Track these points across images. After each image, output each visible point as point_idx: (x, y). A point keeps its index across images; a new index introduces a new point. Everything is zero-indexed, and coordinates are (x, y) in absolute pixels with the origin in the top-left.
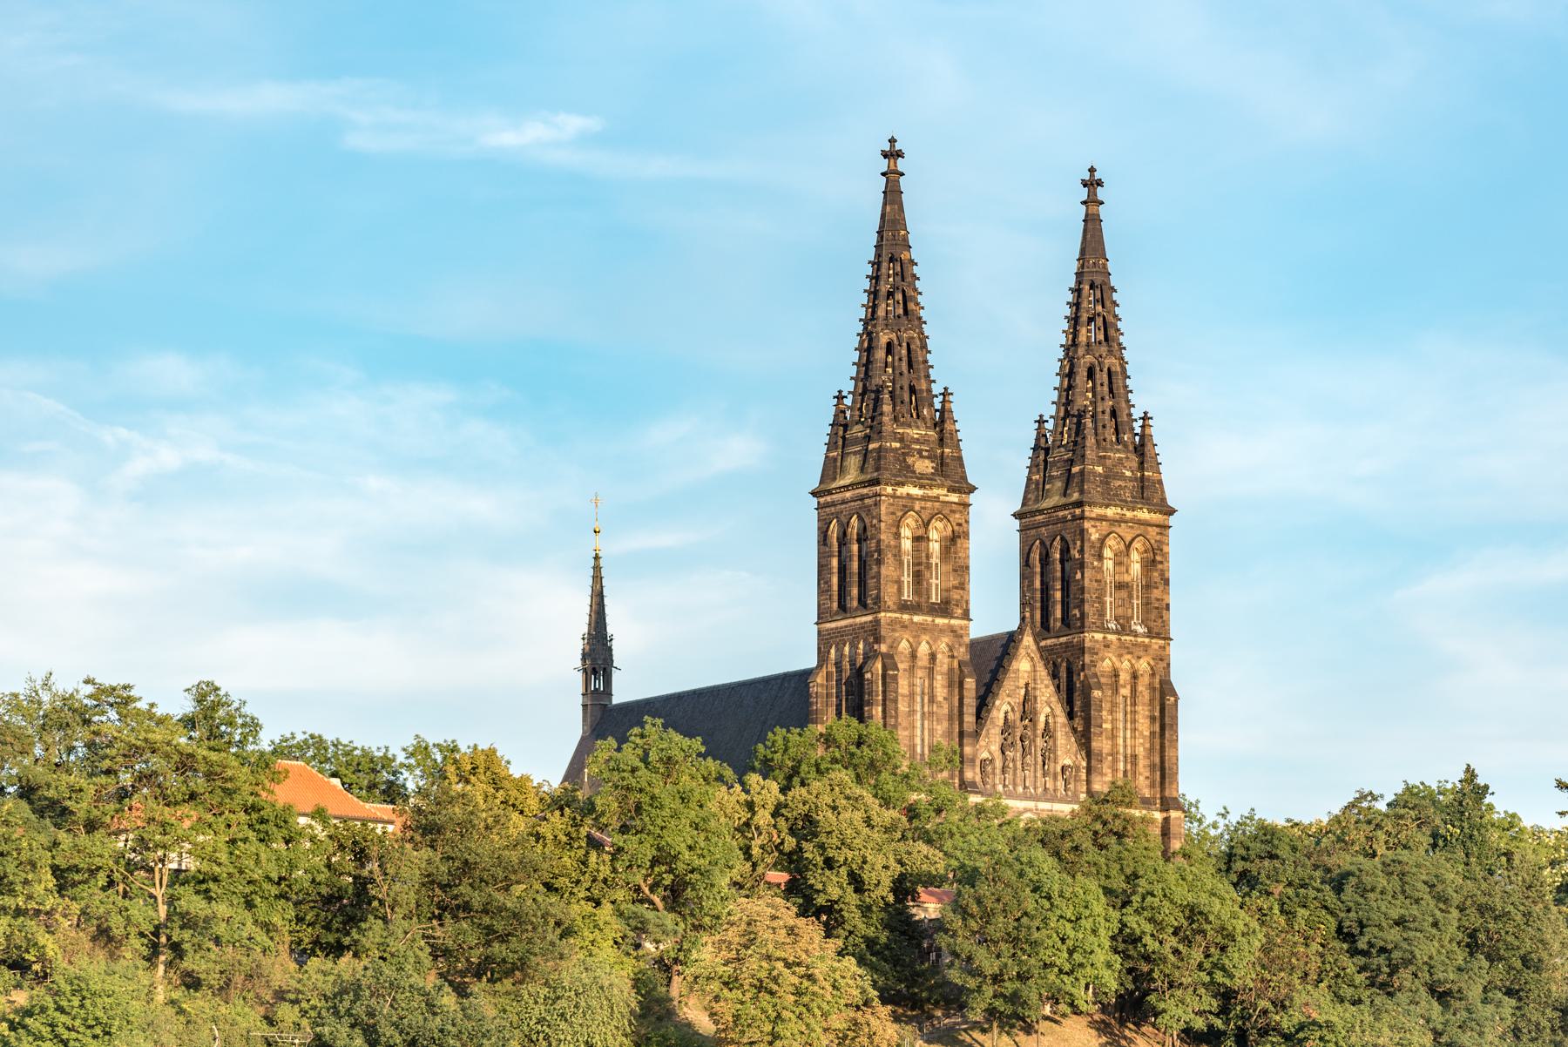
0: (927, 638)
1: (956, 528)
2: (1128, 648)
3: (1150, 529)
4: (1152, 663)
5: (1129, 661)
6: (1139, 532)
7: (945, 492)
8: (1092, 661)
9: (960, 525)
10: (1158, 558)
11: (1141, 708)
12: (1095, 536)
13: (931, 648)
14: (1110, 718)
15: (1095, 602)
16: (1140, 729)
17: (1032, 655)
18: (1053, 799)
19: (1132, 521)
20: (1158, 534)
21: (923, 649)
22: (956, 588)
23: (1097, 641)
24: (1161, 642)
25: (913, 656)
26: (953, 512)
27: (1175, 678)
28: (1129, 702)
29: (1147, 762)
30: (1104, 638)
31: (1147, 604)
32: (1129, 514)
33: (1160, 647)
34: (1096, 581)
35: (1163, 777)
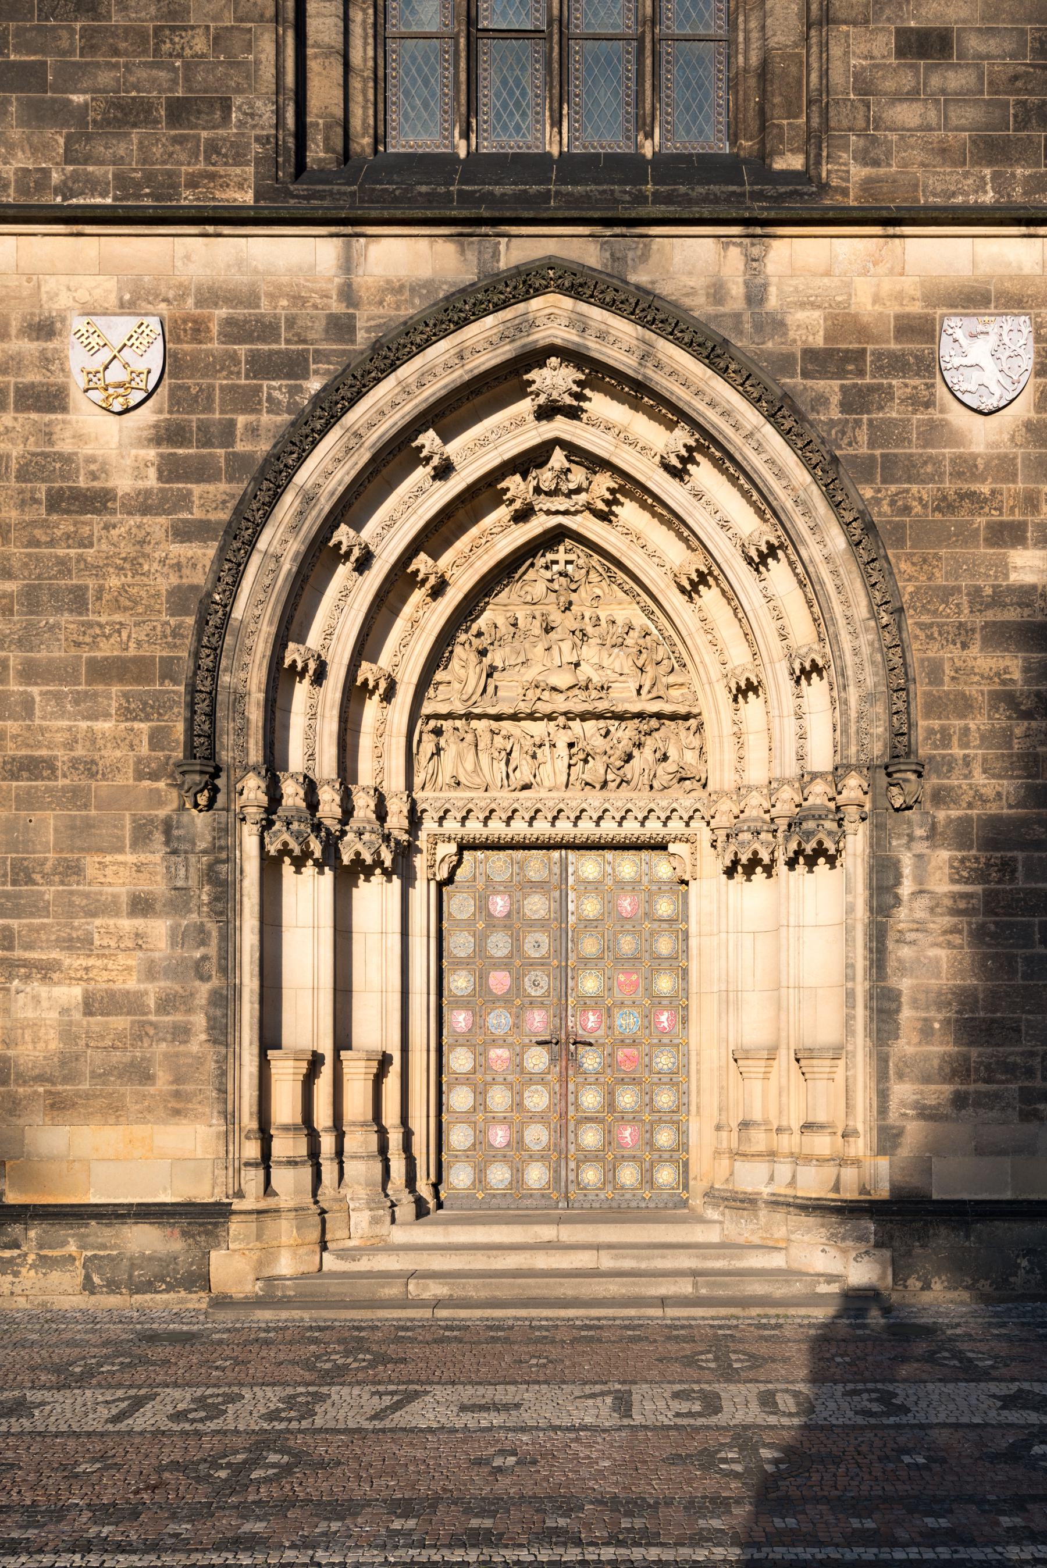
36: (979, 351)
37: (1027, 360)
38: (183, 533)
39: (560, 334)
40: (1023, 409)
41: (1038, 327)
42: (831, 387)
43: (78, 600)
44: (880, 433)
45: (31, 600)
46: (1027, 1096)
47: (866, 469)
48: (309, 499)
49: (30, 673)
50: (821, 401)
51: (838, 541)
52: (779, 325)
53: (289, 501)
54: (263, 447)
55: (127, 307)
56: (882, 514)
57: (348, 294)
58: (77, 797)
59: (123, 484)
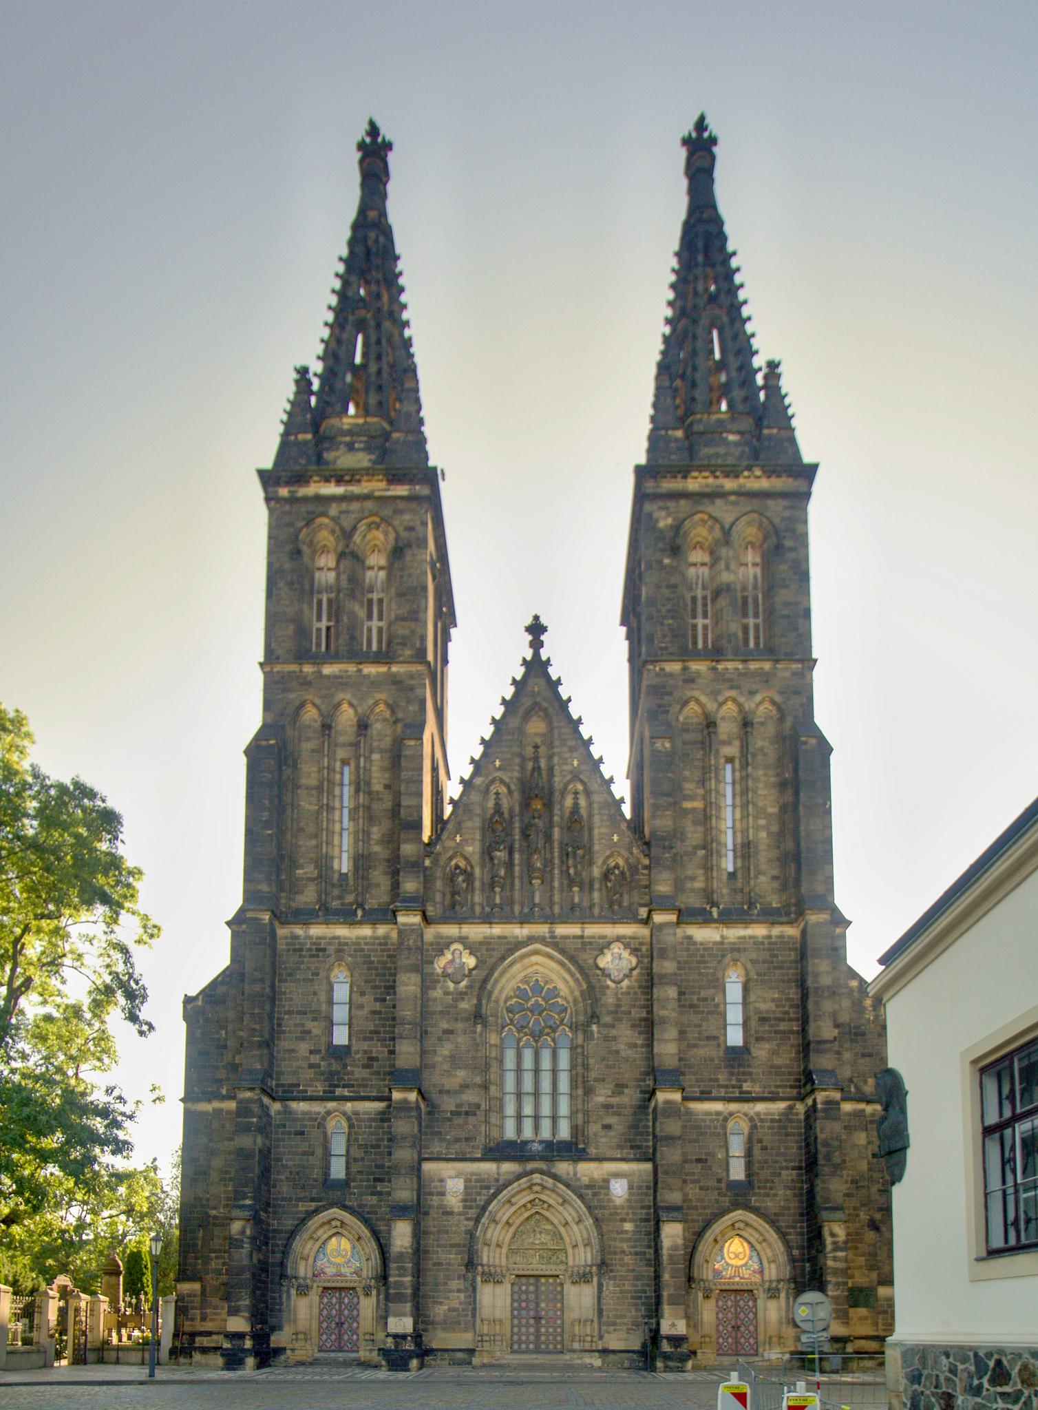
0: (348, 696)
1: (404, 534)
2: (730, 680)
3: (771, 503)
4: (778, 699)
5: (734, 700)
6: (749, 508)
7: (383, 485)
8: (660, 706)
9: (411, 529)
10: (788, 543)
11: (761, 772)
12: (665, 522)
13: (356, 711)
14: (701, 792)
15: (665, 617)
16: (760, 804)
17: (545, 704)
18: (587, 917)
19: (740, 493)
20: (786, 508)
21: (347, 717)
22: (403, 619)
23: (671, 675)
24: (796, 666)
25: (326, 727)
26: (398, 512)
27: (824, 717)
28: (737, 766)
29: (774, 854)
30: (685, 669)
31: (770, 614)
32: (729, 484)
33: (794, 674)
34: (668, 587)
35: (799, 868)
36: (617, 1186)
37: (626, 1187)
38: (467, 1219)
39: (539, 1181)
40: (626, 1196)
41: (629, 1182)
42: (590, 1192)
43: (447, 1232)
44: (599, 1201)
45: (439, 1232)
46: (628, 1329)
47: (596, 1208)
48: (491, 1212)
49: (438, 1246)
50: (587, 1195)
51: (591, 1221)
52: (579, 1180)
53: (487, 1213)
54: (482, 1203)
55: (457, 1177)
56: (600, 1216)
57: (498, 1174)
58: (447, 1270)
59: (456, 1210)
